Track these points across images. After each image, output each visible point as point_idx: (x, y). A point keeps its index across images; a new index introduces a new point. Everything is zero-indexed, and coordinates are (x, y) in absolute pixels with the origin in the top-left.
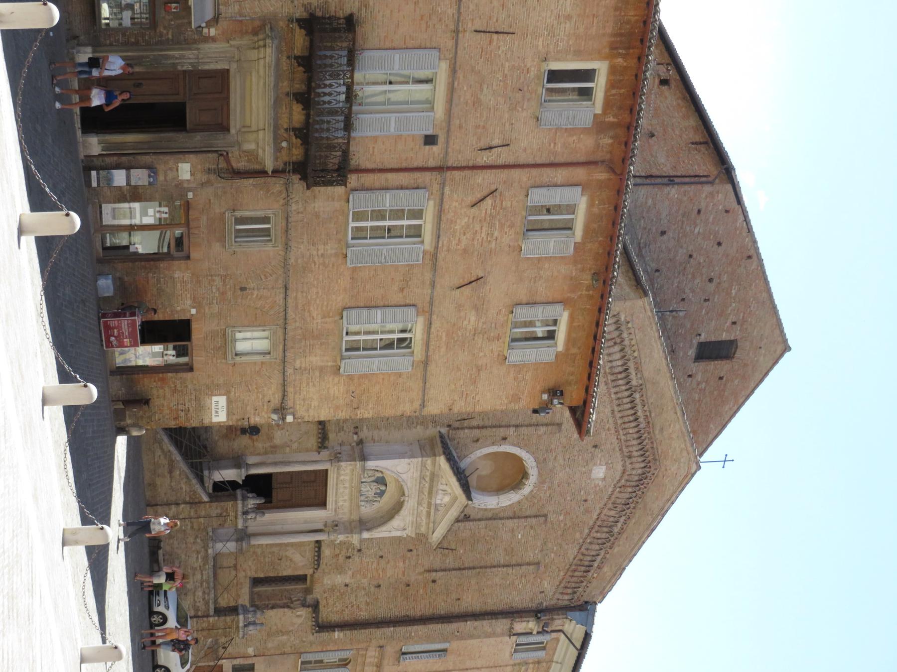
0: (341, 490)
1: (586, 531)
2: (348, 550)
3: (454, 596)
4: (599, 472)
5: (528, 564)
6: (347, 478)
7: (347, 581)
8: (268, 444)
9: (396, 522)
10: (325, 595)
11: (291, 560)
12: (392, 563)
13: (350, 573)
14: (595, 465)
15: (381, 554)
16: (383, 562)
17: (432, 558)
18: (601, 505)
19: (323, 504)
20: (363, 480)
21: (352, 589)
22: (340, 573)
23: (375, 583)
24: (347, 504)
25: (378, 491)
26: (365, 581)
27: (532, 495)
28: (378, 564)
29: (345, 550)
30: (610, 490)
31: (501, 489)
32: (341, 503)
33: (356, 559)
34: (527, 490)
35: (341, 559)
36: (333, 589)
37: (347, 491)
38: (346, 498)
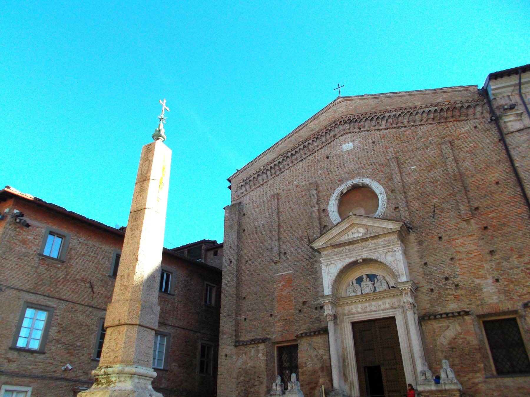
0: (373, 308)
1: (403, 129)
2: (447, 289)
3: (494, 188)
4: (348, 146)
5: (441, 150)
6: (360, 306)
7: (490, 281)
8: (320, 373)
9: (388, 259)
10: (516, 297)
11: (454, 339)
12: (460, 249)
13: (477, 281)
14: (342, 151)
15: (448, 261)
16: (458, 257)
17: (448, 220)
18: (377, 133)
19: (392, 319)
20: (359, 293)
21: (501, 275)
22: (481, 289)
23: (489, 257)
24: (388, 301)
25: (368, 279)
26: (487, 266)
27: (373, 176)
28: (460, 260)
29: (449, 291)
30: (363, 133)
31: (375, 196)
32: (387, 306)
33: (459, 278)
34: (367, 181)
35: (459, 292)
36: (506, 292)
37: (373, 303)
38: (380, 303)
